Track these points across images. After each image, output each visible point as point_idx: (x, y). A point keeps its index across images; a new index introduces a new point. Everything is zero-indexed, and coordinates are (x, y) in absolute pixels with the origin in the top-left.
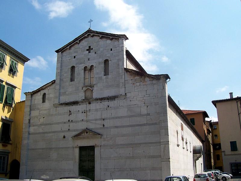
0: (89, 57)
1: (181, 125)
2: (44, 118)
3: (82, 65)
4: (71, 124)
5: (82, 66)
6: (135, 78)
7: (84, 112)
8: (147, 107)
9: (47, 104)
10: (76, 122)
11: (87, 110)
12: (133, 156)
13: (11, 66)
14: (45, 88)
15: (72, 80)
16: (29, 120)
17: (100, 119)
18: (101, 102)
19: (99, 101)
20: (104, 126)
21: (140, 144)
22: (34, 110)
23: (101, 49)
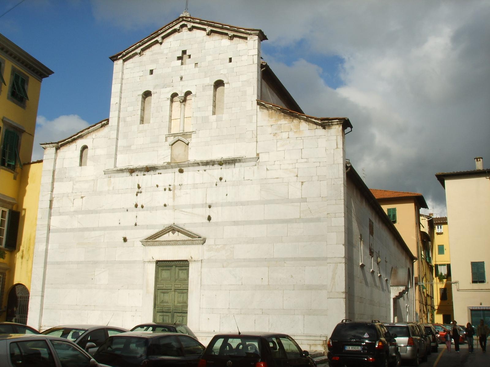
0: (182, 73)
1: (370, 224)
2: (82, 197)
3: (168, 89)
4: (141, 213)
6: (279, 123)
7: (170, 190)
8: (302, 184)
9: (91, 170)
10: (153, 209)
11: (174, 185)
12: (270, 284)
13: (13, 85)
15: (142, 121)
16: (51, 201)
17: (203, 205)
18: (205, 171)
19: (202, 168)
20: (209, 218)
21: (285, 260)
22: (61, 180)
23: (209, 58)
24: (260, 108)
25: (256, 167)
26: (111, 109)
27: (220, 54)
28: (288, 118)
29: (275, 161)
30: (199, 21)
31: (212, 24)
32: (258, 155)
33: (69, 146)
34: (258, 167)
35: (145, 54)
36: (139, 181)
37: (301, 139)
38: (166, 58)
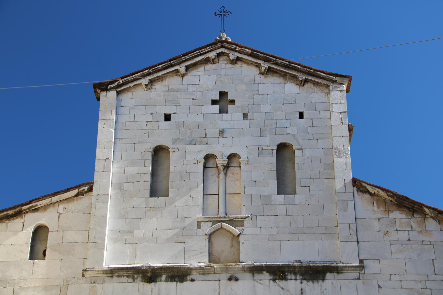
0: (222, 125)
3: (198, 147)
5: (200, 151)
6: (392, 215)
14: (45, 207)
23: (266, 109)
24: (357, 191)
25: (360, 281)
26: (96, 168)
27: (283, 104)
28: (405, 210)
29: (391, 275)
30: (250, 51)
31: (272, 58)
32: (361, 261)
33: (6, 222)
34: (363, 282)
35: (155, 89)
36: (152, 291)
37: (429, 243)
38: (193, 99)
